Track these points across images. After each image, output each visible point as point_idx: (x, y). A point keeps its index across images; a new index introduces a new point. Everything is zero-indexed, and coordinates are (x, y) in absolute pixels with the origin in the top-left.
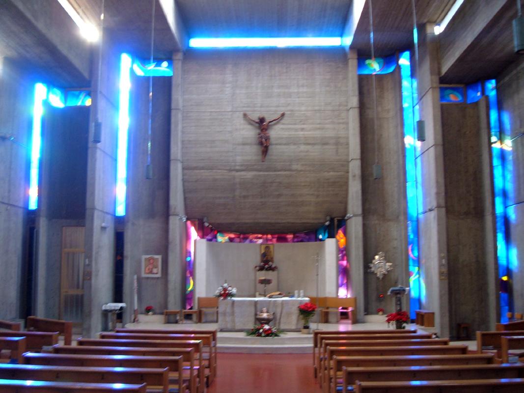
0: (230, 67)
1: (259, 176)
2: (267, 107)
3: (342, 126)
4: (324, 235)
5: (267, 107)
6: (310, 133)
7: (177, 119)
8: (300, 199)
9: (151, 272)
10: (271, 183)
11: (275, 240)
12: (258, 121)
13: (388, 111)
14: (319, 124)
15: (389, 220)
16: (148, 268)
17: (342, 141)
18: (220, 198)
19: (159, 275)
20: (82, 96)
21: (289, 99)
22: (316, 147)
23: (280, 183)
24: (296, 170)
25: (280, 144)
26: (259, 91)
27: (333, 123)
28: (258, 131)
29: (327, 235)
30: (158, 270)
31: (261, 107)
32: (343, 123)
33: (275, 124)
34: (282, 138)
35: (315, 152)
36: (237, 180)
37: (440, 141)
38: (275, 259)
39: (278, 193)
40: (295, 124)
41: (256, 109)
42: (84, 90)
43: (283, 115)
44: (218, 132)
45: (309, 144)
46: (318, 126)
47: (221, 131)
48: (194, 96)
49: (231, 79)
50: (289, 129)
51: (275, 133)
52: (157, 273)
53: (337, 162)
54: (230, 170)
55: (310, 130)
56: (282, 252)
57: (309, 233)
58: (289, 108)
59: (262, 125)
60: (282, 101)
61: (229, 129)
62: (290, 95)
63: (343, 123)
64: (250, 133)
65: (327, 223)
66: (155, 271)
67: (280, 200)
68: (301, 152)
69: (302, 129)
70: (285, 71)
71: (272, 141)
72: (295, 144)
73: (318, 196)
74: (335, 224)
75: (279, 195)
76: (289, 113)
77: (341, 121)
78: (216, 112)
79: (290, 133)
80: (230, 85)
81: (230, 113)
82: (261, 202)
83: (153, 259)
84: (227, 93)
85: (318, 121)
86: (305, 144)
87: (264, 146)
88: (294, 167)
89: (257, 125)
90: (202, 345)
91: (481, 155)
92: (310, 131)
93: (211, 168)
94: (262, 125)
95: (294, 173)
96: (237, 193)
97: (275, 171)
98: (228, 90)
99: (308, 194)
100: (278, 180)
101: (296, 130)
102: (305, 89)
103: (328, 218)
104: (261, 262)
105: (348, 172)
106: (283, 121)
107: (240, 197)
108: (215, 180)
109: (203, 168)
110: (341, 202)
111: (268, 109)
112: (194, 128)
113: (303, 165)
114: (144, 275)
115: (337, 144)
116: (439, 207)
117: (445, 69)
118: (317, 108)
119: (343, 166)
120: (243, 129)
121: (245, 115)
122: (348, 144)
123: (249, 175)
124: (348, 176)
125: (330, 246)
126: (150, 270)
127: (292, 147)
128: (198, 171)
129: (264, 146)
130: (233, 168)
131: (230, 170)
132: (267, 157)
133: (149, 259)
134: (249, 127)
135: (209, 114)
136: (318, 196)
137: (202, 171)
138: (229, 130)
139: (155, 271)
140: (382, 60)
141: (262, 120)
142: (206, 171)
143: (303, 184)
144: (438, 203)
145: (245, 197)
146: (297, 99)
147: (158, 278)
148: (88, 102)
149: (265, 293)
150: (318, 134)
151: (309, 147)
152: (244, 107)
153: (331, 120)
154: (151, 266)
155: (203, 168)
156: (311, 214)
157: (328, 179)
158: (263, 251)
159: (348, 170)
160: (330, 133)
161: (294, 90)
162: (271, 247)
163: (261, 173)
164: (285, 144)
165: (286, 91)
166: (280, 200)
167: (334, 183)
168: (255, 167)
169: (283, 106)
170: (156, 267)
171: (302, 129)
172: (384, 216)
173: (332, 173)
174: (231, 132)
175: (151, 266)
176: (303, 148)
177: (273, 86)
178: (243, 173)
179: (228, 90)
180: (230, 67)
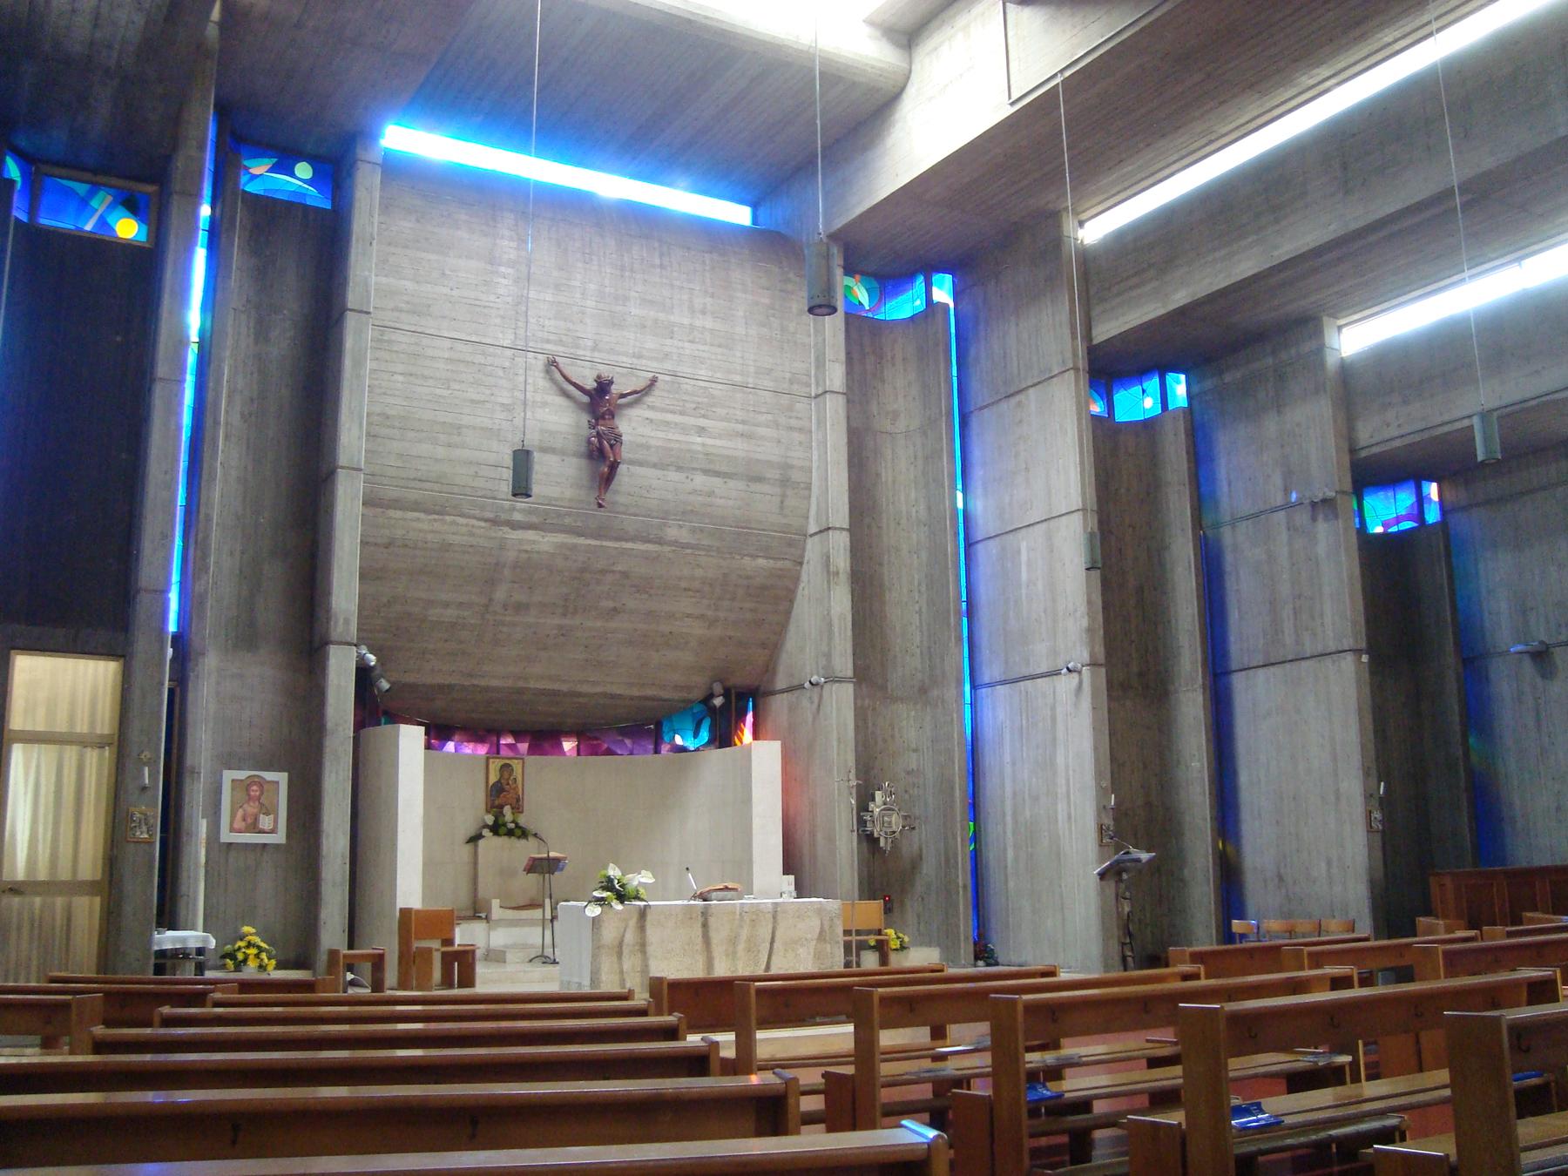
0: (509, 218)
1: (574, 547)
2: (611, 351)
3: (797, 436)
4: (696, 735)
5: (611, 351)
6: (718, 442)
7: (357, 338)
8: (665, 628)
9: (254, 827)
10: (603, 572)
11: (523, 747)
12: (590, 384)
13: (895, 416)
14: (743, 422)
15: (895, 700)
16: (240, 813)
17: (796, 476)
18: (446, 605)
19: (280, 838)
20: (100, 202)
21: (669, 342)
22: (732, 483)
23: (625, 575)
24: (675, 543)
25: (641, 464)
26: (589, 303)
27: (777, 425)
28: (585, 418)
29: (705, 735)
30: (276, 821)
31: (595, 348)
32: (801, 430)
33: (630, 405)
34: (648, 447)
35: (728, 496)
36: (511, 555)
37: (1092, 503)
38: (529, 803)
39: (611, 604)
40: (682, 413)
41: (581, 352)
42: (111, 187)
43: (654, 381)
44: (472, 401)
45: (717, 474)
46: (740, 427)
47: (479, 402)
48: (409, 285)
49: (513, 255)
50: (667, 423)
51: (632, 426)
52: (273, 831)
53: (965, 511)
54: (495, 522)
55: (720, 437)
56: (558, 783)
57: (632, 726)
58: (668, 366)
59: (599, 400)
60: (651, 343)
61: (504, 397)
62: (669, 331)
63: (801, 430)
64: (559, 421)
65: (718, 701)
66: (265, 822)
67: (612, 625)
68: (694, 492)
69: (701, 431)
70: (657, 261)
71: (625, 452)
72: (679, 469)
73: (713, 623)
74: (728, 708)
75: (615, 609)
76: (668, 378)
77: (793, 422)
78: (1127, 278)
79: (670, 436)
80: (510, 271)
81: (509, 353)
82: (561, 627)
83: (261, 783)
84: (501, 291)
85: (740, 414)
86: (706, 472)
87: (602, 457)
88: (672, 533)
89: (586, 399)
90: (683, 1027)
91: (1167, 548)
92: (717, 439)
93: (437, 509)
94: (599, 400)
95: (667, 549)
96: (500, 594)
97: (618, 539)
98: (505, 285)
99: (688, 616)
100: (619, 568)
101: (684, 429)
102: (709, 323)
103: (718, 688)
104: (488, 811)
105: (801, 564)
106: (649, 400)
107: (505, 607)
108: (446, 547)
109: (416, 506)
110: (763, 645)
111: (618, 354)
112: (400, 378)
113: (693, 530)
114: (226, 836)
115: (785, 482)
116: (1093, 664)
117: (1105, 330)
118: (738, 378)
119: (791, 543)
120: (545, 404)
121: (552, 363)
122: (809, 487)
123: (545, 542)
124: (799, 573)
125: (763, 756)
126: (249, 821)
127: (673, 475)
128: (398, 514)
129: (602, 457)
130: (503, 517)
131: (495, 522)
132: (608, 496)
133: (251, 782)
134: (561, 401)
135: (448, 343)
136: (713, 623)
137: (410, 515)
138: (505, 401)
139: (265, 822)
140: (875, 284)
141: (603, 387)
142: (422, 516)
143: (683, 584)
144: (1092, 655)
145: (520, 608)
146: (687, 345)
147: (277, 846)
148: (128, 229)
149: (476, 911)
150: (739, 448)
151: (717, 481)
152: (548, 341)
153: (770, 417)
154: (251, 808)
155: (416, 506)
156: (678, 669)
157: (748, 578)
158: (493, 779)
159: (802, 556)
160: (769, 452)
161: (681, 318)
162: (516, 765)
163: (582, 541)
164: (655, 466)
165: (662, 316)
166: (612, 625)
167: (763, 588)
168: (567, 521)
169: (651, 359)
170: (270, 810)
171: (701, 431)
172: (883, 688)
173: (761, 562)
174: (507, 408)
175: (251, 808)
176: (700, 480)
177: (626, 299)
178: (531, 535)
179: (505, 285)
180: (509, 218)
